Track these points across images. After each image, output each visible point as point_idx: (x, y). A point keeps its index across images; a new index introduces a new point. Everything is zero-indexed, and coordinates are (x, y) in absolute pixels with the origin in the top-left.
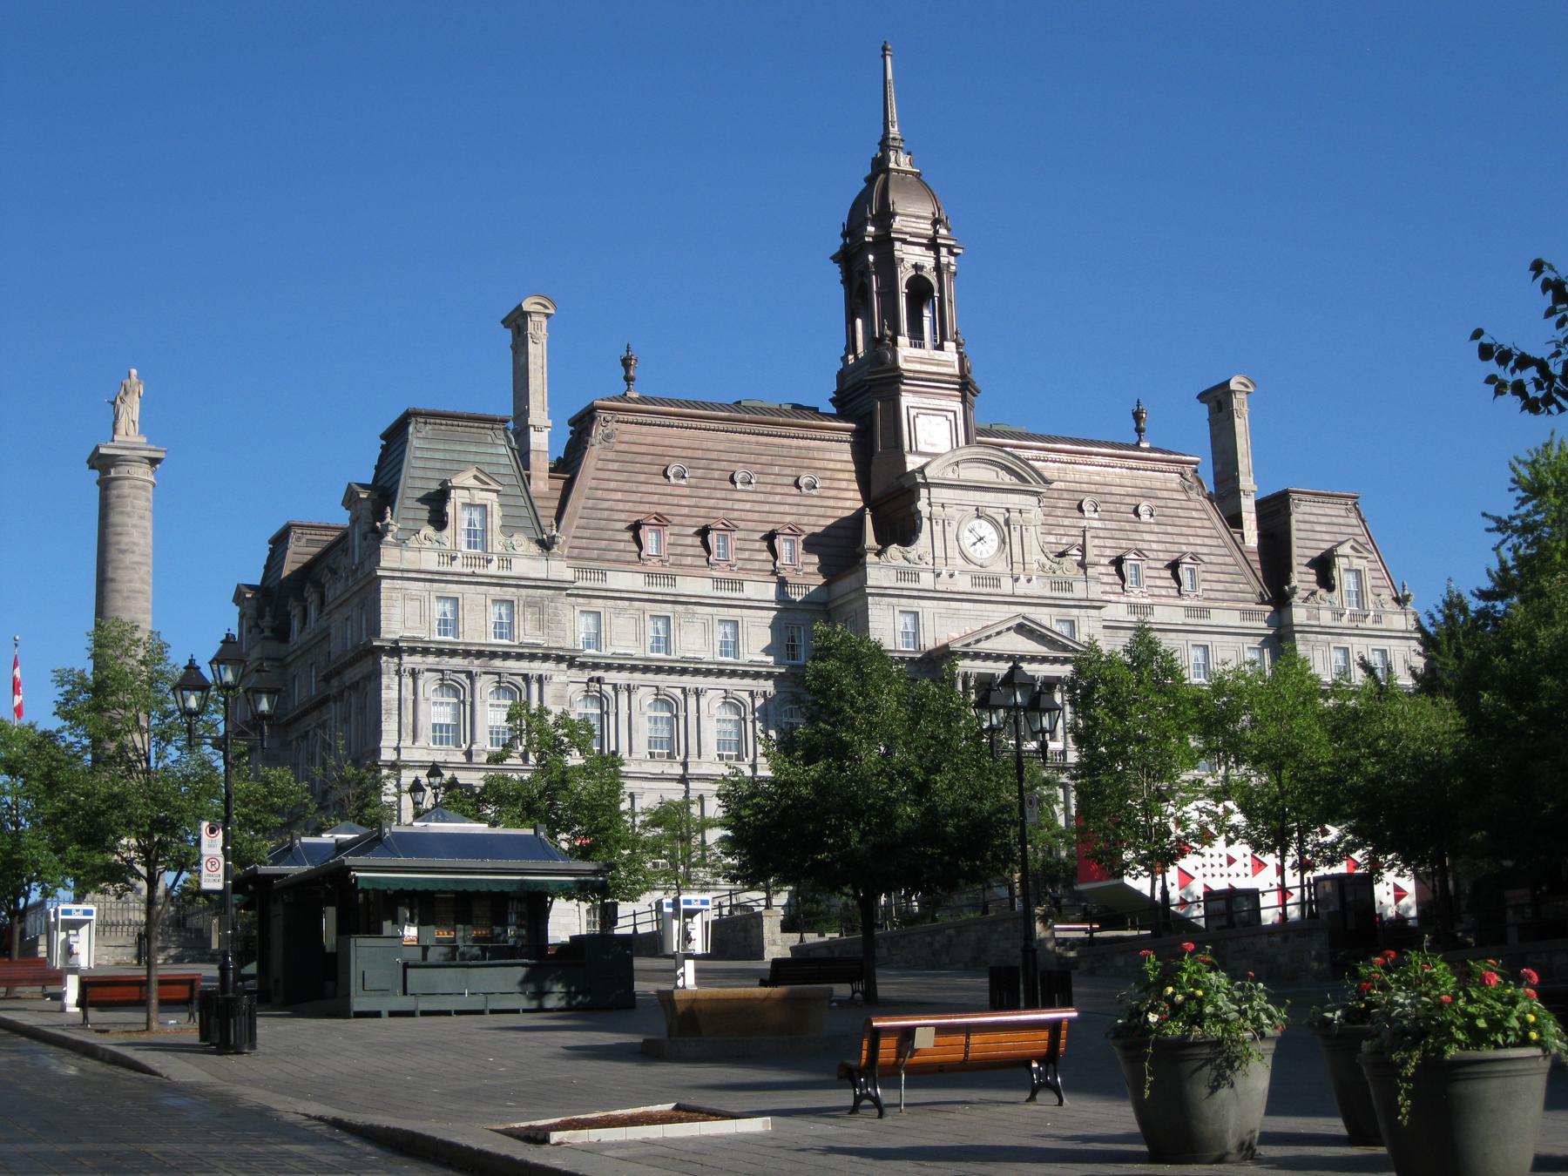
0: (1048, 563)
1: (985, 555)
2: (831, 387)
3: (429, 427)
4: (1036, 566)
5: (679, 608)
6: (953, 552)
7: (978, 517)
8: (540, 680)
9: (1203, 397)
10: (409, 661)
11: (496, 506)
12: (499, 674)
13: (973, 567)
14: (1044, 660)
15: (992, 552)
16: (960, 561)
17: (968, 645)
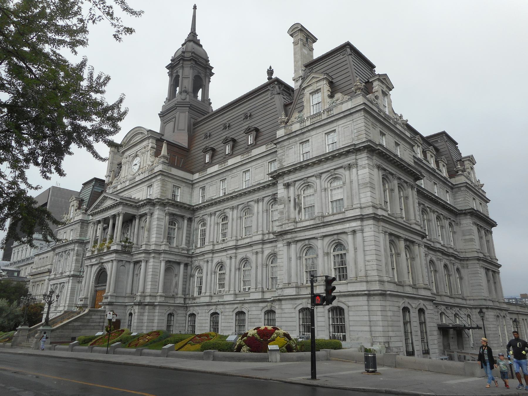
8: (72, 250)
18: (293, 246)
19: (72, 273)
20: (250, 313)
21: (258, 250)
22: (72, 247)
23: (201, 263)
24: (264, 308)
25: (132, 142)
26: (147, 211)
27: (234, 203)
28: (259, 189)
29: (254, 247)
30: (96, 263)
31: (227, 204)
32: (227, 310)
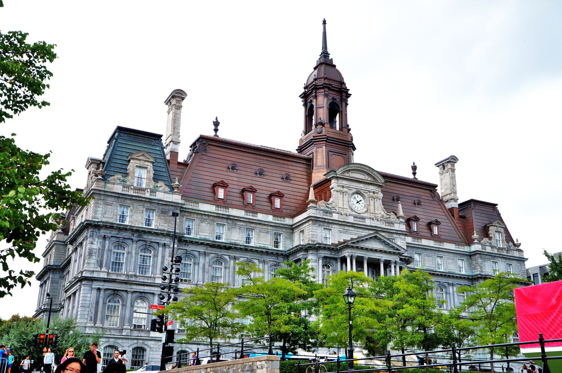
0: (385, 215)
1: (359, 209)
2: (297, 145)
3: (126, 135)
4: (380, 215)
5: (230, 221)
6: (346, 206)
7: (358, 193)
8: (164, 245)
9: (438, 165)
10: (103, 232)
11: (152, 169)
12: (146, 241)
13: (354, 213)
14: (385, 252)
15: (362, 208)
16: (349, 211)
17: (354, 243)
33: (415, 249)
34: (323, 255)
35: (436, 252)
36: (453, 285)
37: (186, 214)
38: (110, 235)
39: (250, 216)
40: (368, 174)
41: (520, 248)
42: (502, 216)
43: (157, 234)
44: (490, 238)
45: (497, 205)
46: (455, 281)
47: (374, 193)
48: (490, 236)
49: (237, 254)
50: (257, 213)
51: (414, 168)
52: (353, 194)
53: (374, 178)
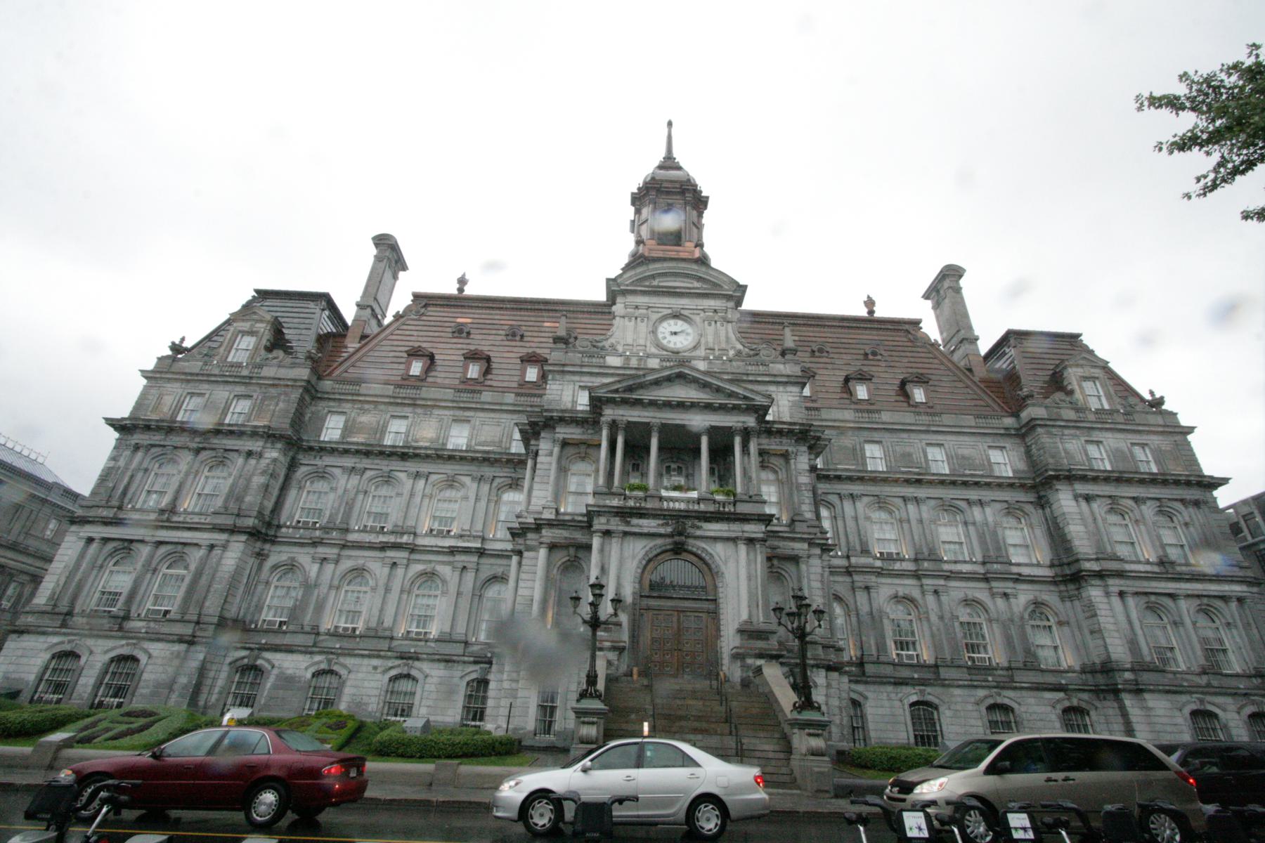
4: (731, 353)
5: (419, 411)
7: (676, 316)
8: (250, 454)
9: (926, 296)
14: (708, 407)
16: (654, 350)
17: (616, 391)
18: (1131, 601)
19: (250, 522)
20: (1023, 709)
21: (1008, 591)
22: (256, 445)
23: (843, 590)
24: (1058, 701)
25: (655, 283)
26: (790, 449)
27: (921, 492)
28: (988, 484)
29: (994, 584)
30: (662, 530)
31: (894, 489)
32: (959, 699)
33: (866, 433)
34: (561, 436)
35: (923, 436)
36: (981, 503)
37: (332, 404)
38: (146, 443)
39: (465, 396)
40: (699, 279)
41: (1164, 407)
42: (1097, 353)
43: (232, 432)
44: (1071, 393)
45: (1079, 335)
46: (986, 495)
47: (715, 311)
48: (1069, 388)
49: (424, 468)
50: (480, 392)
51: (870, 303)
52: (664, 318)
53: (715, 285)
